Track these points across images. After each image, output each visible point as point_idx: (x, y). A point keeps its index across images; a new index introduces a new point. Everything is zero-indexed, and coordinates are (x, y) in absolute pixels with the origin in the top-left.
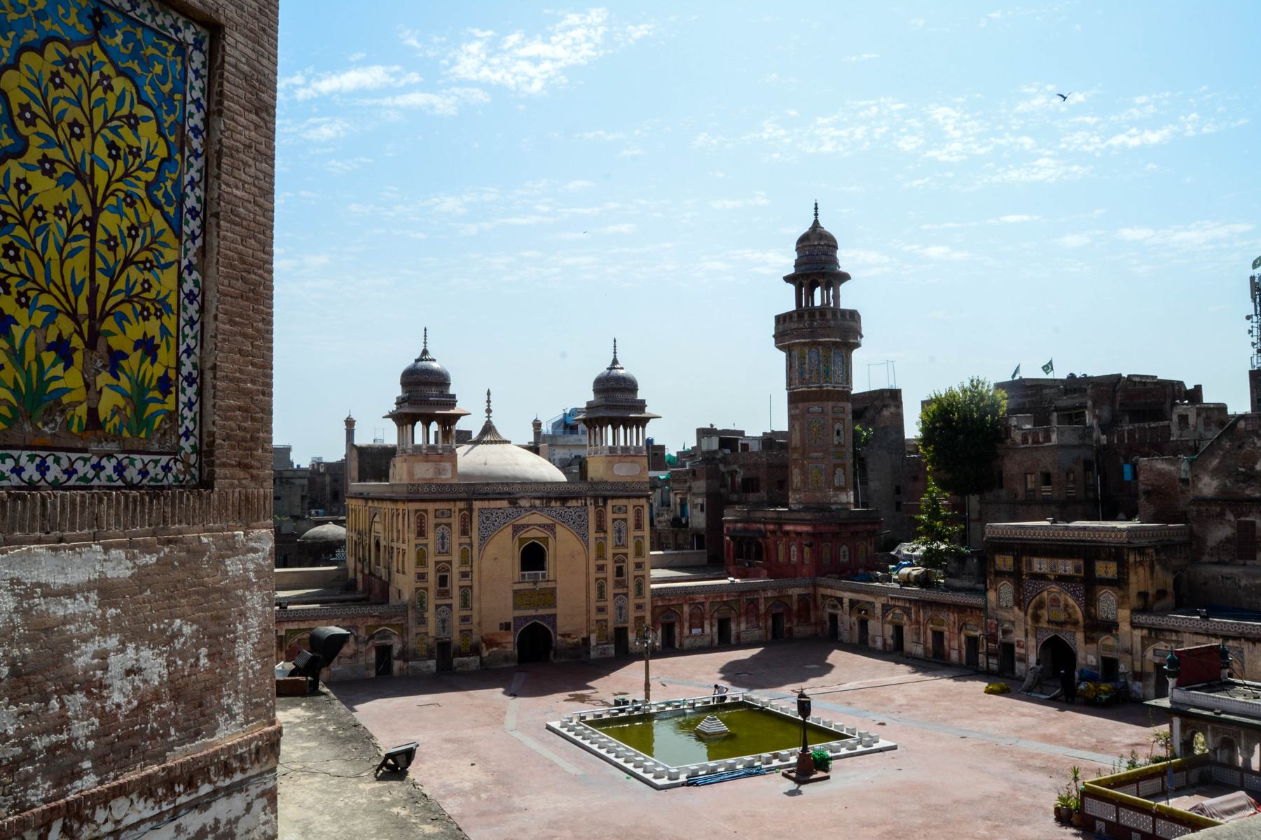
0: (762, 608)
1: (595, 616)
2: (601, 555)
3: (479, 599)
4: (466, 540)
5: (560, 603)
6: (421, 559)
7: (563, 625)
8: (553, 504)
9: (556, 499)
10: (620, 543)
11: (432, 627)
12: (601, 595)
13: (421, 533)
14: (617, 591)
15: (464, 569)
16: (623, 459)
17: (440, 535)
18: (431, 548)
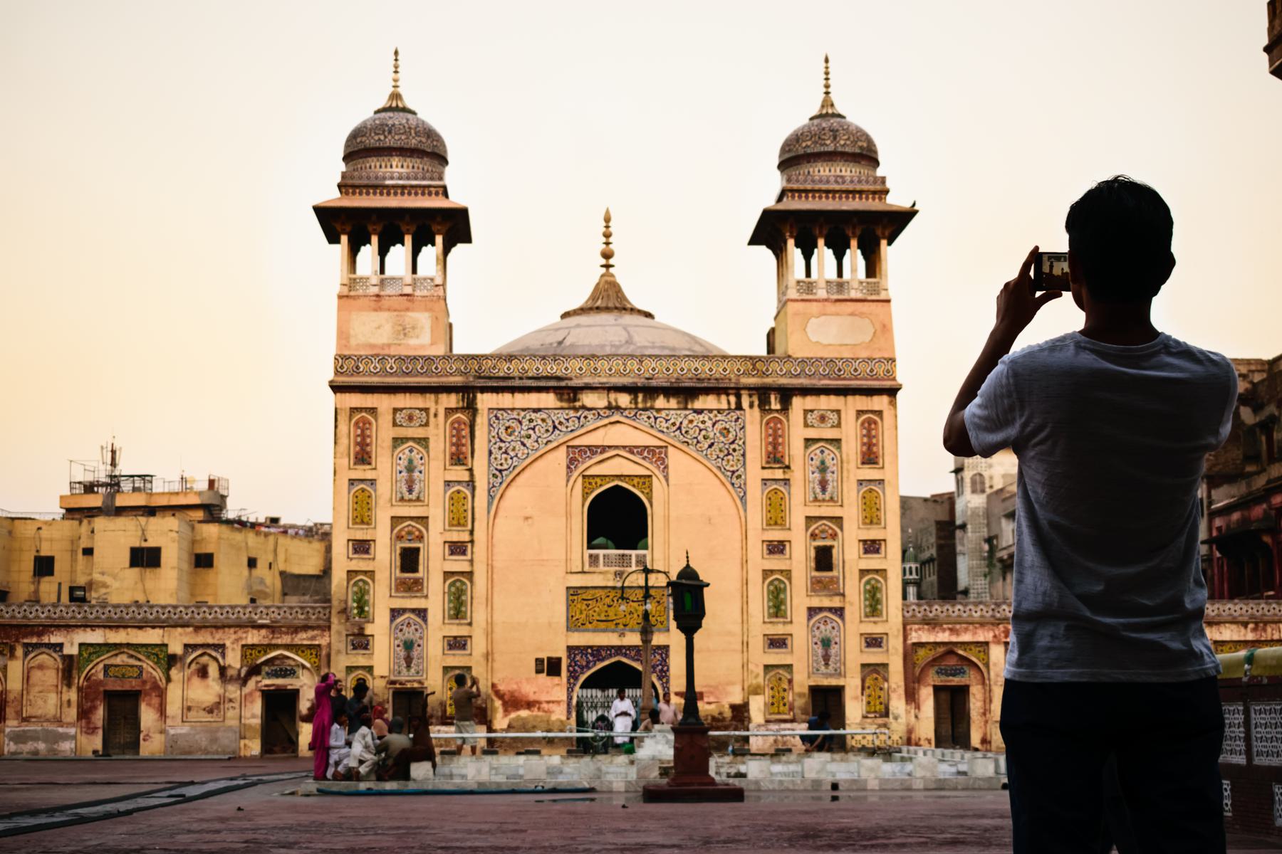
1: (761, 657)
2: (776, 515)
3: (489, 601)
4: (460, 474)
6: (362, 513)
8: (660, 402)
9: (669, 392)
12: (777, 607)
13: (363, 457)
14: (816, 602)
15: (455, 537)
16: (831, 308)
17: (404, 463)
18: (384, 489)
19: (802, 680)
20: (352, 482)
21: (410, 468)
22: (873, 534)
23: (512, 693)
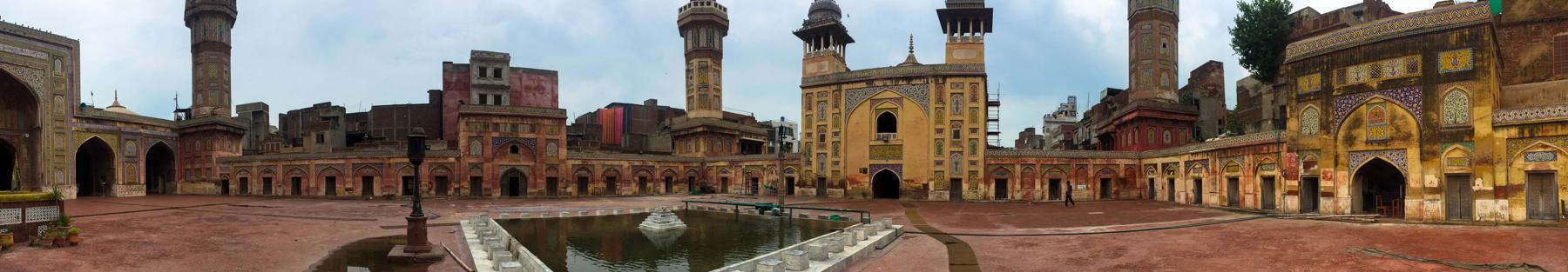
0: (1091, 173)
1: (933, 168)
2: (939, 120)
3: (846, 151)
4: (837, 111)
5: (905, 156)
7: (906, 174)
8: (901, 83)
9: (903, 79)
10: (957, 110)
11: (814, 167)
12: (939, 151)
13: (809, 108)
14: (953, 149)
15: (835, 130)
18: (815, 117)
19: (947, 177)
20: (807, 116)
21: (823, 110)
22: (974, 126)
23: (852, 179)
